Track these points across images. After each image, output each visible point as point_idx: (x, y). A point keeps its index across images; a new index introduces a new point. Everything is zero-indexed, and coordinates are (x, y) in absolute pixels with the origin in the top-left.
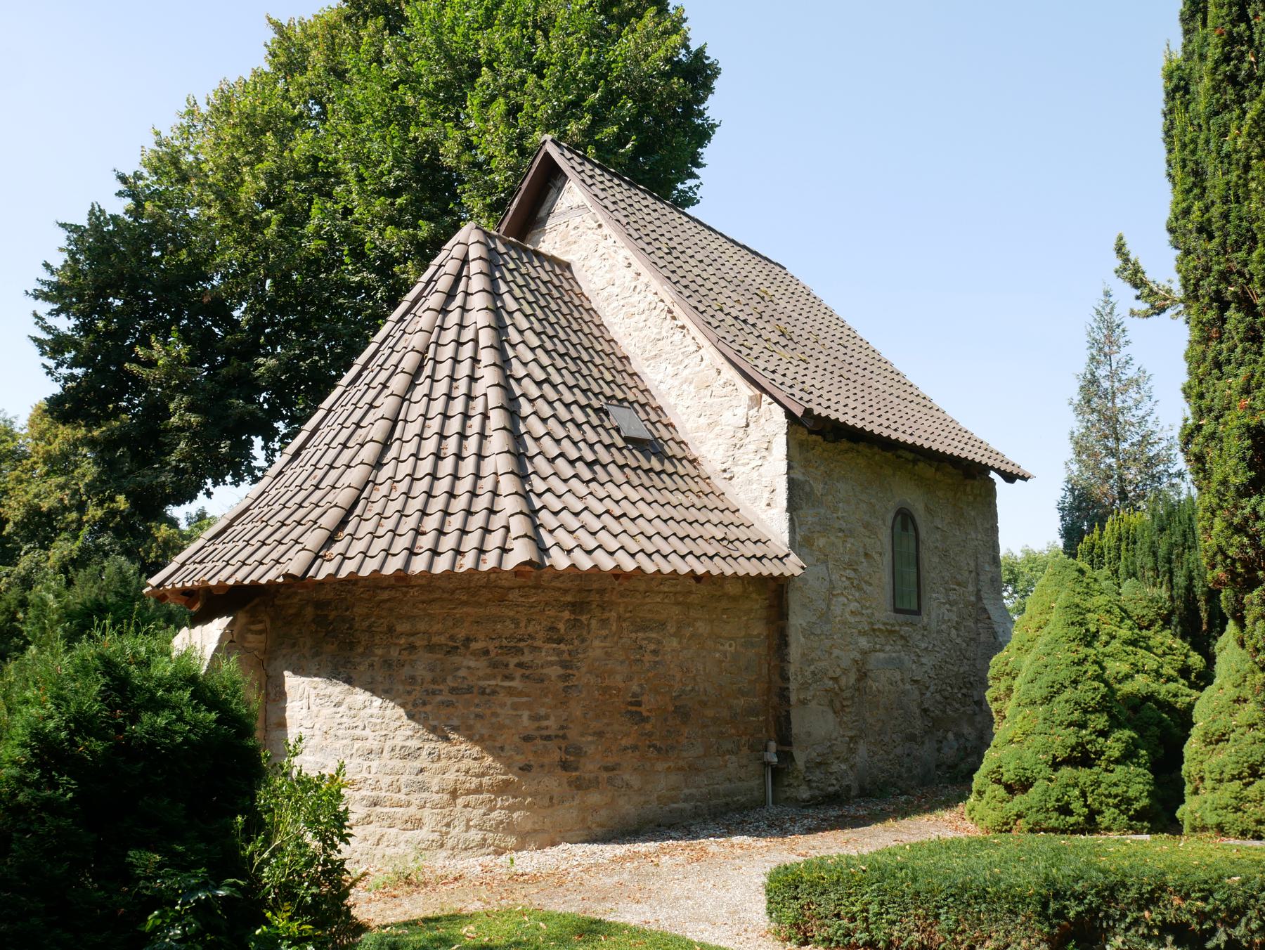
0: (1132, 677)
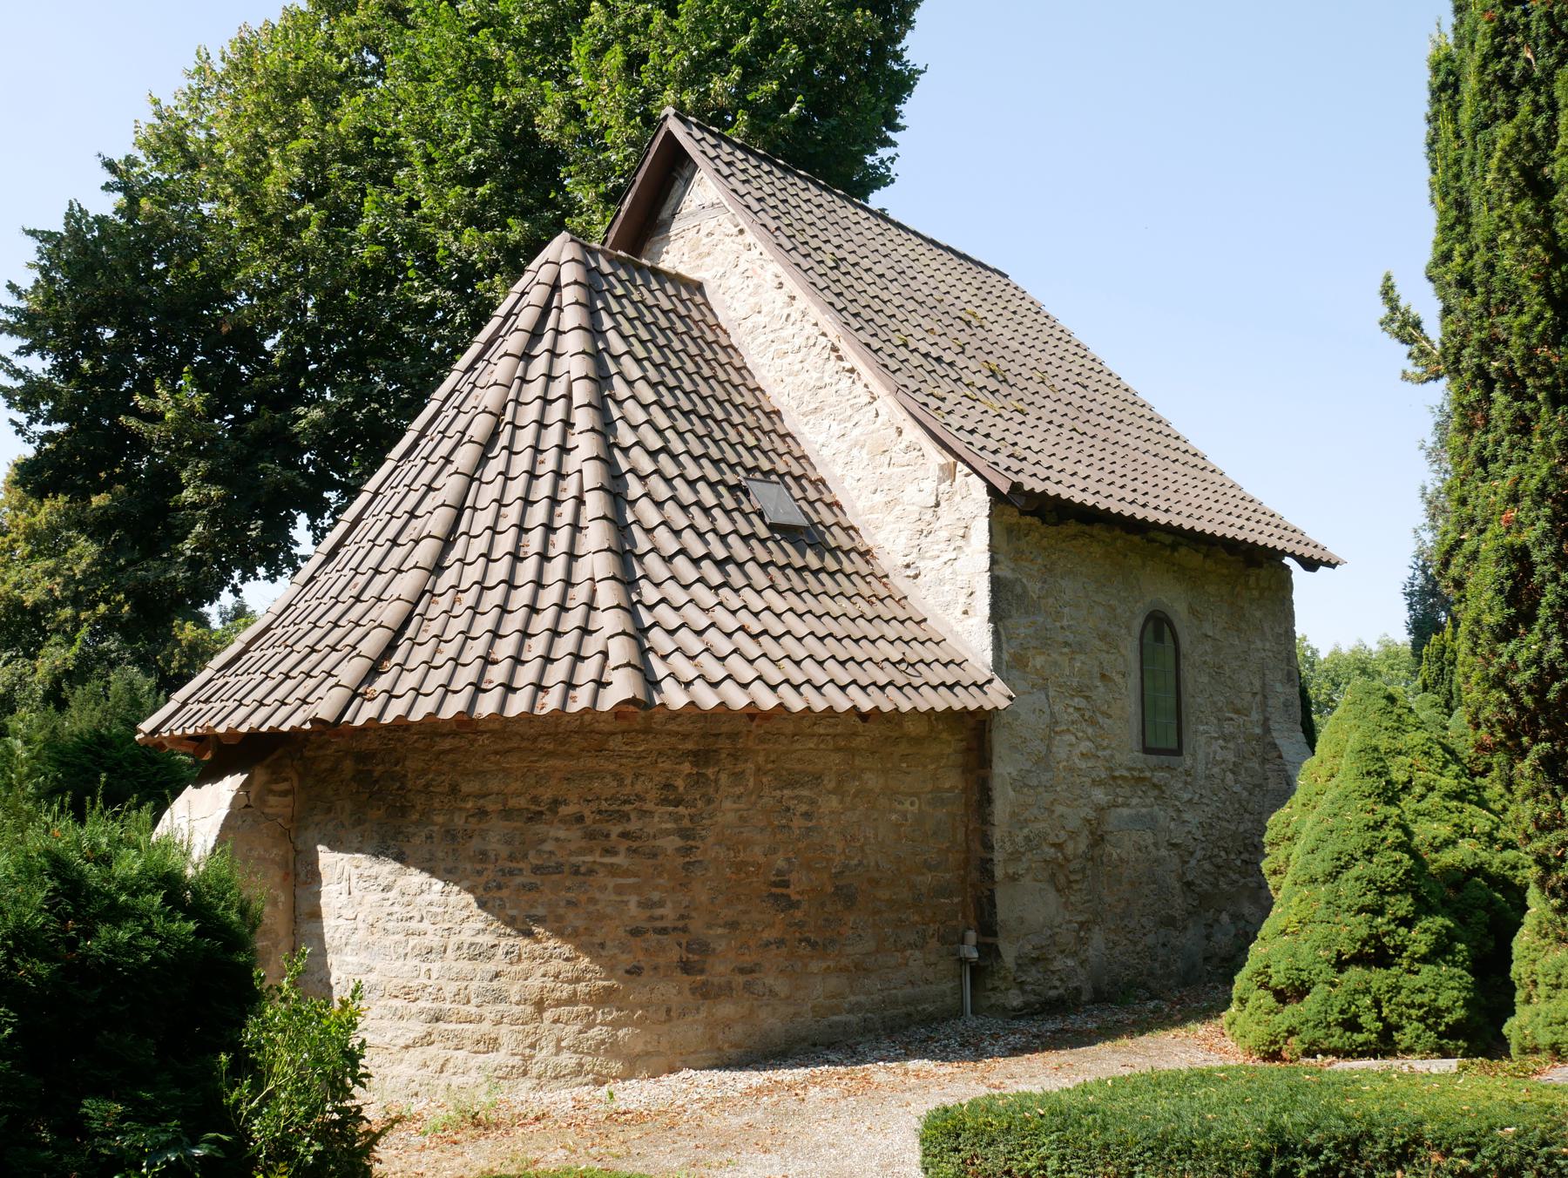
0: (1454, 843)
